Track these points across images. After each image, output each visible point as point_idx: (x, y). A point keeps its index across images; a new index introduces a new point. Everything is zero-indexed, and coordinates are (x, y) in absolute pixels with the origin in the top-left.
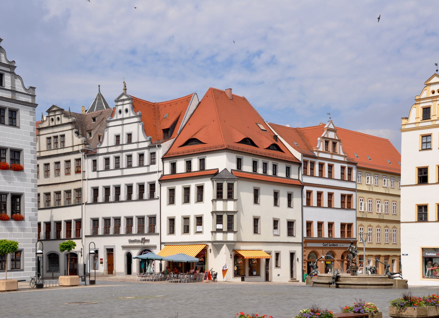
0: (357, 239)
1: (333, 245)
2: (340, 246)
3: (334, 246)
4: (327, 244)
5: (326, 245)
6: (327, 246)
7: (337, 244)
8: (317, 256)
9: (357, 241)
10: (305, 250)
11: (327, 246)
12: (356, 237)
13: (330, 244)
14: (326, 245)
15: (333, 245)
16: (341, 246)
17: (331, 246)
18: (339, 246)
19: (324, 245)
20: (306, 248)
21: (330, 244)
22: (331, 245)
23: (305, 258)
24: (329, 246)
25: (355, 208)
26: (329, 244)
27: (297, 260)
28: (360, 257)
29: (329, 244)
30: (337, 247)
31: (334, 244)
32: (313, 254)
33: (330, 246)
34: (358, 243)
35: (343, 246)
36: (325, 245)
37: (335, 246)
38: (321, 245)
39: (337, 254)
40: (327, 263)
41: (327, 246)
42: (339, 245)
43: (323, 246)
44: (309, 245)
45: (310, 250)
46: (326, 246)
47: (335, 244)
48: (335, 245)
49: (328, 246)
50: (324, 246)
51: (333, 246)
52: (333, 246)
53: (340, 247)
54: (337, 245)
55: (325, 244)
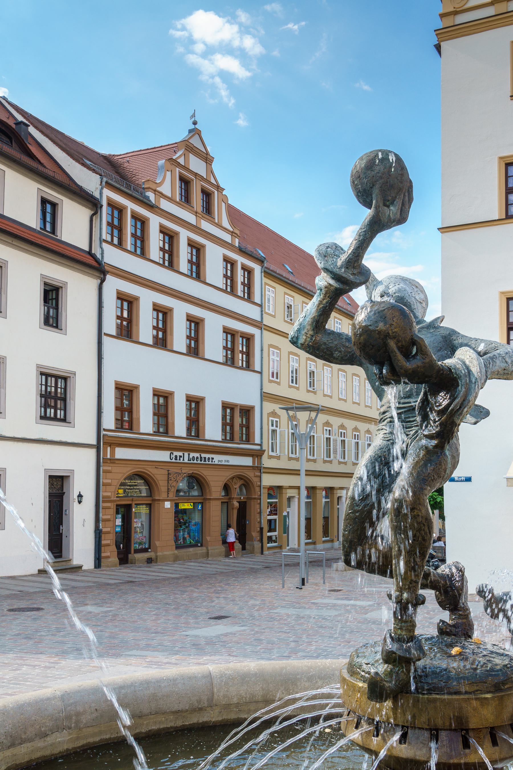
0: (265, 447)
1: (201, 458)
2: (219, 461)
3: (203, 462)
4: (181, 454)
5: (178, 459)
6: (181, 461)
7: (211, 456)
8: (150, 488)
9: (264, 451)
10: (109, 468)
11: (182, 459)
12: (262, 442)
13: (191, 456)
14: (180, 457)
15: (201, 458)
16: (223, 463)
17: (195, 461)
18: (216, 463)
19: (173, 456)
20: (113, 461)
21: (191, 456)
22: (193, 457)
23: (109, 494)
24: (189, 460)
25: (259, 370)
26: (189, 454)
27: (77, 500)
28: (271, 492)
29: (189, 454)
30: (210, 463)
31: (203, 455)
32: (139, 481)
33: (192, 461)
34: (265, 457)
35: (228, 461)
36: (176, 456)
37: (207, 462)
38: (163, 456)
39: (212, 484)
40: (182, 506)
41: (182, 459)
42: (218, 459)
43: (169, 460)
44: (121, 453)
45: (129, 469)
46: (178, 461)
47: (207, 456)
48: (205, 458)
49: (186, 460)
50: (174, 460)
51: (199, 462)
52: (201, 461)
53: (220, 463)
54: (213, 459)
55: (176, 453)
